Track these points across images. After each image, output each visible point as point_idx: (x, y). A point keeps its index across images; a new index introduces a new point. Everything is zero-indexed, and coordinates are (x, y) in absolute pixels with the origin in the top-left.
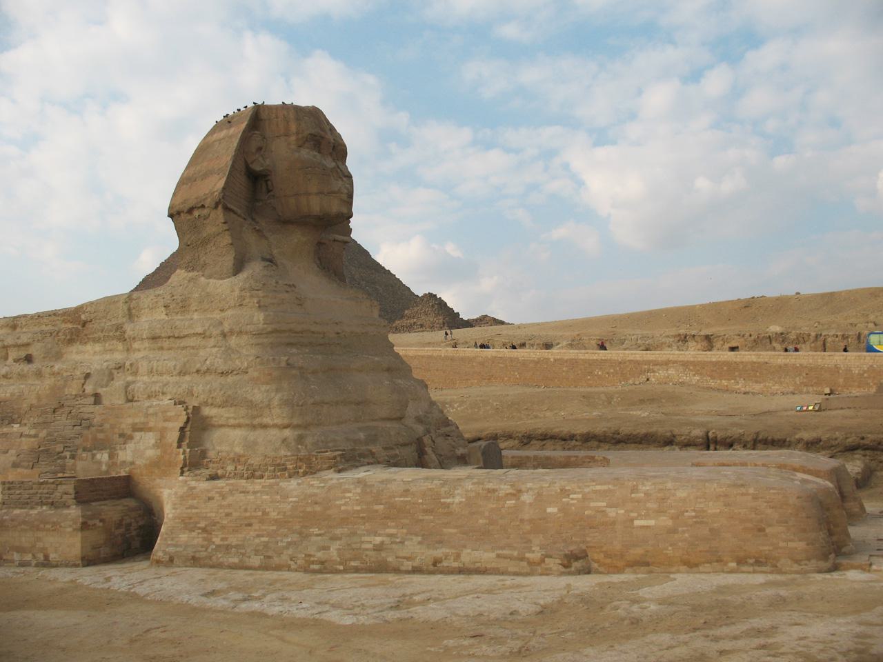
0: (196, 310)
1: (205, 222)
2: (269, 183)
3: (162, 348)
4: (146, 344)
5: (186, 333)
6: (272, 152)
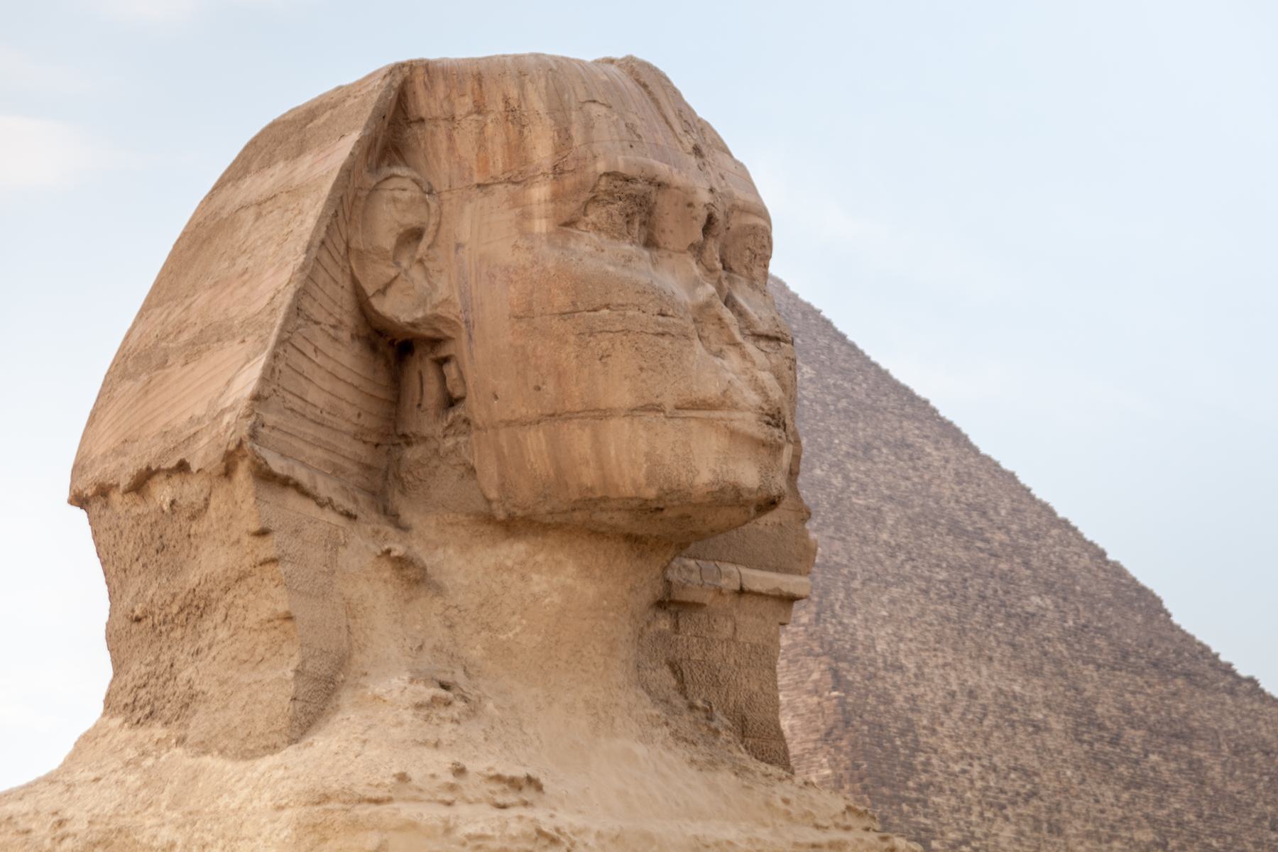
1: (195, 528)
2: (451, 370)
6: (459, 246)
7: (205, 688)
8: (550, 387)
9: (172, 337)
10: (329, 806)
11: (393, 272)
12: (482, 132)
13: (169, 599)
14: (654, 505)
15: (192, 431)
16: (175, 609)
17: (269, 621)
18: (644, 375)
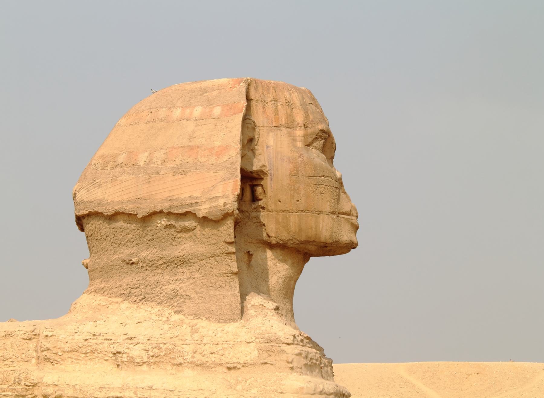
1: (179, 235)
2: (259, 190)
7: (187, 294)
8: (303, 201)
9: (159, 163)
10: (272, 344)
13: (157, 258)
15: (194, 201)
16: (160, 262)
17: (226, 274)
18: (333, 201)
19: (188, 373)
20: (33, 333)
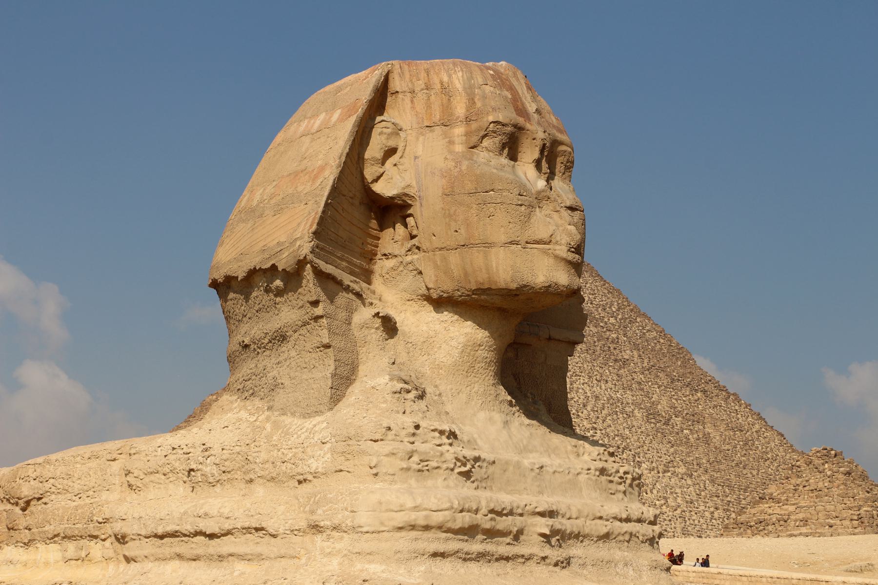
0: (251, 481)
1: (278, 299)
2: (410, 220)
3: (180, 556)
4: (150, 547)
5: (227, 526)
8: (462, 231)
10: (351, 442)
11: (381, 170)
12: (429, 99)
14: (514, 293)
16: (266, 341)
18: (511, 225)
19: (260, 491)
20: (119, 452)
